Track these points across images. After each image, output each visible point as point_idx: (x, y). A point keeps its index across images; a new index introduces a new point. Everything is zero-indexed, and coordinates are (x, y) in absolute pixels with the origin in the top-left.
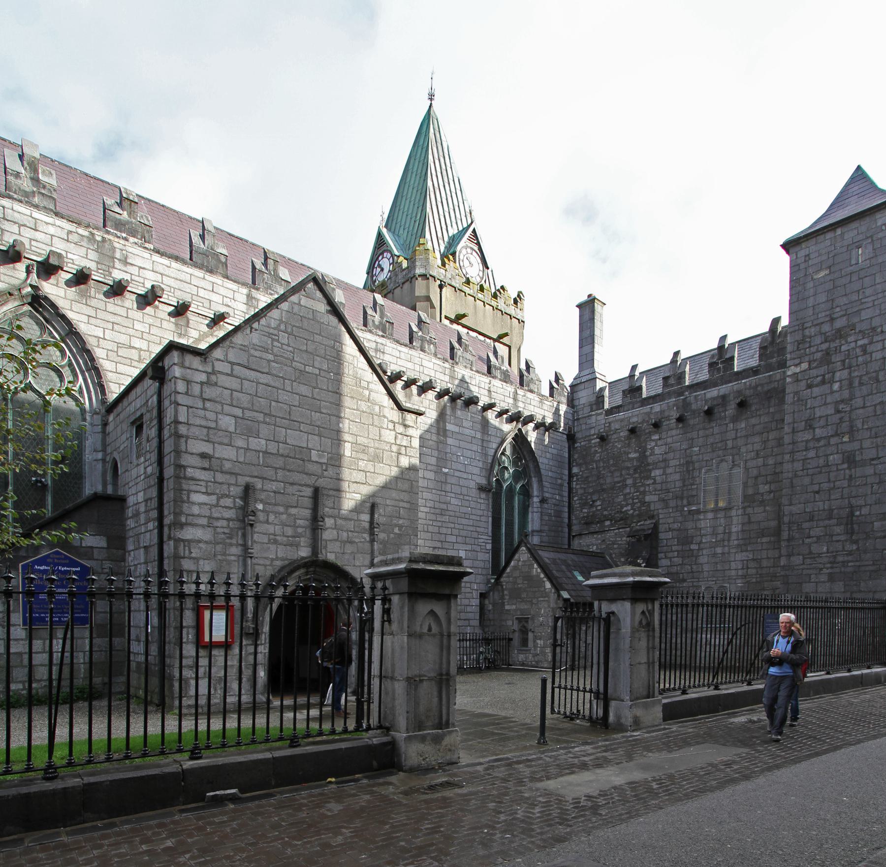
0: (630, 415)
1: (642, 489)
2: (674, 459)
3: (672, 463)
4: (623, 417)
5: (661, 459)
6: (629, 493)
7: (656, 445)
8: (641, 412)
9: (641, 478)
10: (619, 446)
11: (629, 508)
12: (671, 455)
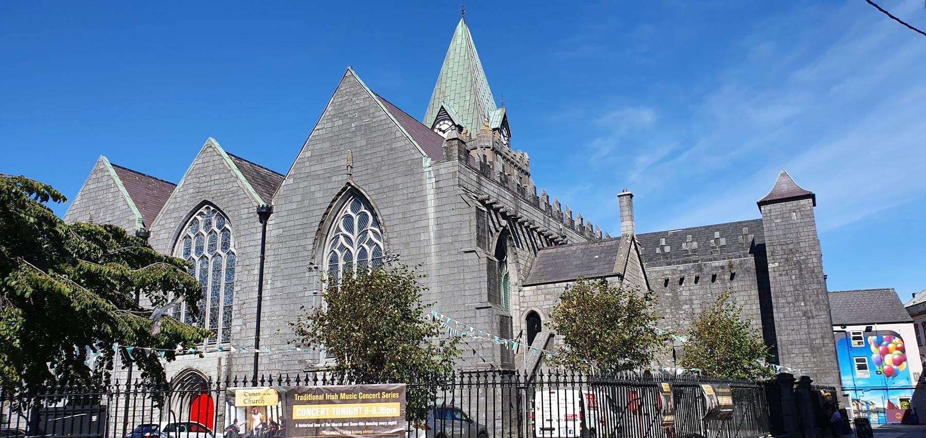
0: (664, 269)
1: (677, 316)
2: (696, 300)
3: (695, 302)
4: (659, 269)
5: (688, 299)
6: (669, 318)
7: (683, 290)
8: (671, 268)
9: (676, 309)
10: (658, 287)
11: (670, 327)
12: (694, 297)
